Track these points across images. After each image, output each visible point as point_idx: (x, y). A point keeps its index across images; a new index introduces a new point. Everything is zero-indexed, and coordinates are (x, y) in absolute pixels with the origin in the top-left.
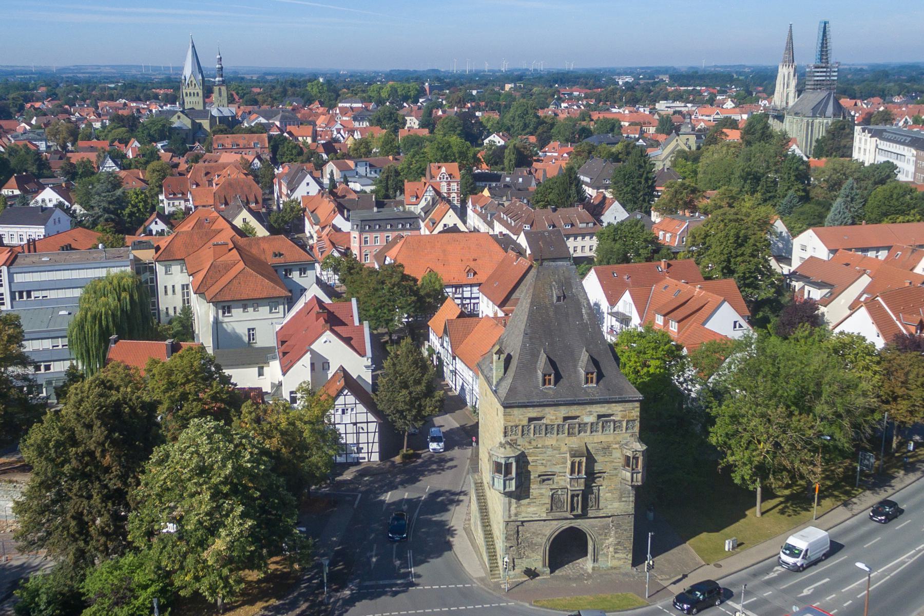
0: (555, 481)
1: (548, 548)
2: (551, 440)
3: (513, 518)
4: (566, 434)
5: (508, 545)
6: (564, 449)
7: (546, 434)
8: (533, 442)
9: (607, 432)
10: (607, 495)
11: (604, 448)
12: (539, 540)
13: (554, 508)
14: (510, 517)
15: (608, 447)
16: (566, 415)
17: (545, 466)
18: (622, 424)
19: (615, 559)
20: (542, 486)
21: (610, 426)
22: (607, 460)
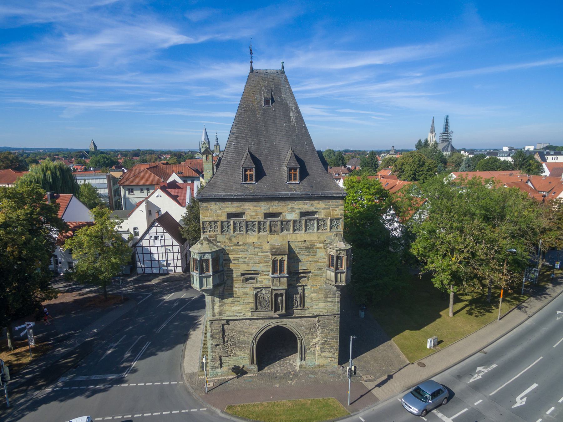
0: (259, 280)
1: (255, 346)
2: (252, 238)
3: (217, 317)
4: (268, 232)
5: (214, 343)
6: (267, 247)
7: (247, 231)
9: (311, 231)
10: (312, 295)
11: (307, 247)
12: (246, 338)
13: (259, 307)
14: (214, 316)
15: (313, 246)
16: (267, 211)
17: (248, 265)
18: (326, 223)
20: (245, 285)
21: (313, 224)
22: (311, 260)
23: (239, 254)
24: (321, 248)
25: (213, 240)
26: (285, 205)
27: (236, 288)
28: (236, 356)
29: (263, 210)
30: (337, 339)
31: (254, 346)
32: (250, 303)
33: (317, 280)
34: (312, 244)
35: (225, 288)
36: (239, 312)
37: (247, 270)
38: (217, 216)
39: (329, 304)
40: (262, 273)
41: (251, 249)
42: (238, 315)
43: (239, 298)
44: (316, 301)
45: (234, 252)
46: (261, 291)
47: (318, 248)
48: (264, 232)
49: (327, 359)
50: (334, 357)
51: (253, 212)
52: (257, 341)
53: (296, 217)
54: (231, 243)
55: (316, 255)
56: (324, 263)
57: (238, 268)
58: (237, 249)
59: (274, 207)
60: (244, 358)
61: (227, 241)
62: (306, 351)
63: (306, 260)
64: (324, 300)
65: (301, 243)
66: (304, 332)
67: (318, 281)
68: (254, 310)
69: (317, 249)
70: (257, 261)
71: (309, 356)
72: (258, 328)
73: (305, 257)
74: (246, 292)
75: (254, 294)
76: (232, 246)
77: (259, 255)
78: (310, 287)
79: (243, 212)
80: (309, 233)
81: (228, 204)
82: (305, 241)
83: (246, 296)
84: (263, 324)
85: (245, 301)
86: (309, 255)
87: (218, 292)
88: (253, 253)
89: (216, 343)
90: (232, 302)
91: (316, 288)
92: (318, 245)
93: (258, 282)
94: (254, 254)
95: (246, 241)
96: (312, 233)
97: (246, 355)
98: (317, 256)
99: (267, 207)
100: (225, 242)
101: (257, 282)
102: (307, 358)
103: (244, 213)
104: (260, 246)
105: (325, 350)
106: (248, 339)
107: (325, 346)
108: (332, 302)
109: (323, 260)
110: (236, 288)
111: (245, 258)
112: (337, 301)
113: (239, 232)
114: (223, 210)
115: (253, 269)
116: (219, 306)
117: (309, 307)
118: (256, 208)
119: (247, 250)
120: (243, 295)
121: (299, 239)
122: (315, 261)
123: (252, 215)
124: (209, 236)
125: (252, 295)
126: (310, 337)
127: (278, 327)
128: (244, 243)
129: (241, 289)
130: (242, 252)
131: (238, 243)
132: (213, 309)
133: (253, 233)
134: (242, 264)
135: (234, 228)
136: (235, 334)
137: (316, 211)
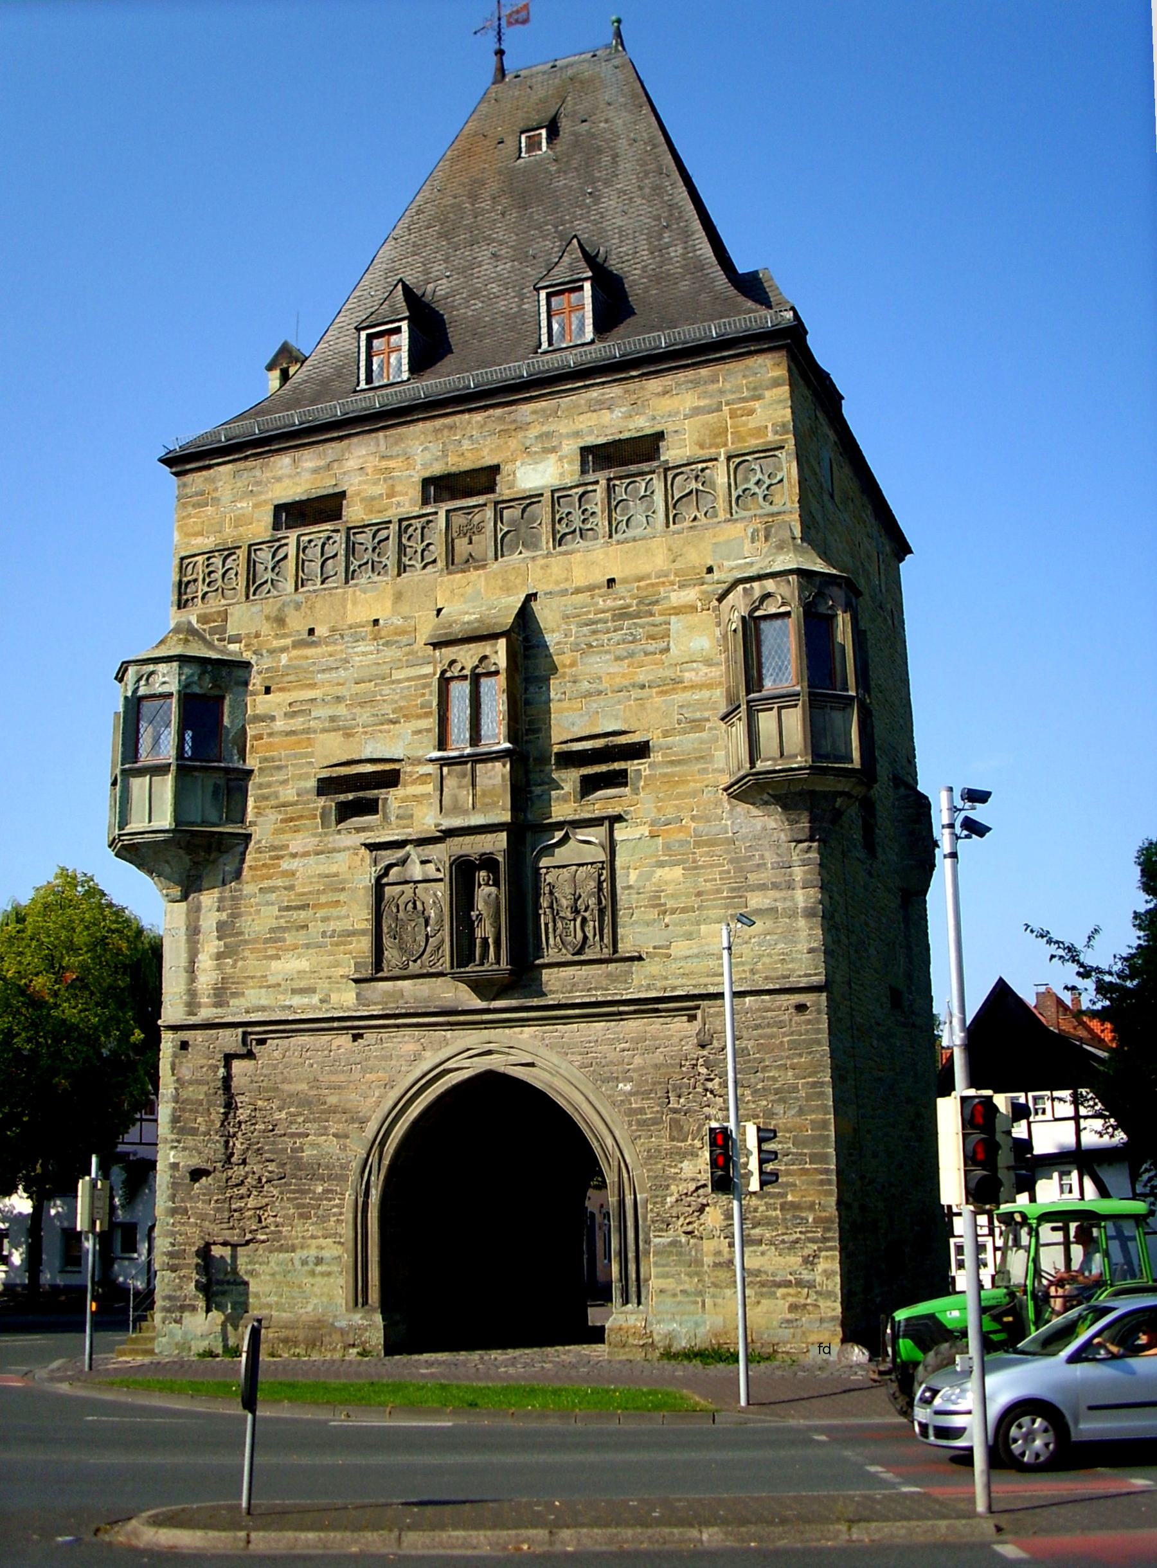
3: (206, 1013)
4: (441, 564)
8: (290, 612)
10: (659, 872)
11: (622, 614)
12: (331, 1145)
15: (648, 604)
16: (437, 469)
17: (348, 735)
22: (642, 677)
23: (313, 686)
24: (693, 609)
25: (213, 631)
26: (513, 427)
27: (294, 856)
28: (281, 1249)
29: (418, 467)
30: (823, 1158)
31: (373, 1191)
32: (353, 933)
34: (645, 594)
35: (248, 858)
36: (303, 984)
37: (344, 759)
38: (238, 522)
40: (409, 769)
41: (364, 654)
42: (297, 1001)
44: (684, 910)
45: (291, 678)
46: (403, 862)
47: (678, 611)
48: (424, 567)
49: (773, 1295)
50: (811, 1285)
51: (376, 483)
52: (386, 1162)
53: (562, 474)
54: (284, 636)
55: (667, 650)
56: (709, 686)
57: (307, 755)
58: (304, 662)
59: (466, 445)
60: (319, 1261)
61: (266, 629)
62: (648, 1242)
64: (727, 907)
65: (592, 596)
66: (632, 1112)
68: (368, 972)
69: (673, 619)
70: (387, 709)
71: (665, 1276)
72: (389, 1085)
73: (615, 668)
74: (336, 875)
75: (373, 881)
76: (284, 649)
77: (399, 681)
78: (645, 830)
79: (337, 490)
80: (626, 541)
81: (284, 462)
82: (611, 582)
84: (417, 1058)
85: (333, 925)
86: (631, 655)
88: (375, 671)
89: (196, 1162)
91: (681, 836)
92: (673, 596)
93: (393, 819)
94: (377, 677)
95: (344, 616)
96: (644, 538)
99: (435, 448)
100: (257, 636)
101: (386, 817)
102: (654, 1284)
103: (343, 494)
104: (404, 632)
105: (757, 1231)
106: (343, 1148)
108: (772, 911)
109: (705, 669)
110: (294, 856)
111: (339, 699)
112: (801, 905)
113: (319, 586)
114: (261, 493)
115: (366, 754)
116: (219, 956)
117: (646, 949)
118: (392, 464)
120: (324, 892)
121: (580, 578)
123: (373, 499)
124: (198, 616)
125: (362, 892)
126: (666, 1144)
127: (490, 1079)
128: (333, 630)
129: (312, 860)
131: (311, 631)
132: (191, 970)
133: (376, 578)
134: (324, 730)
135: (300, 565)
136: (283, 1115)
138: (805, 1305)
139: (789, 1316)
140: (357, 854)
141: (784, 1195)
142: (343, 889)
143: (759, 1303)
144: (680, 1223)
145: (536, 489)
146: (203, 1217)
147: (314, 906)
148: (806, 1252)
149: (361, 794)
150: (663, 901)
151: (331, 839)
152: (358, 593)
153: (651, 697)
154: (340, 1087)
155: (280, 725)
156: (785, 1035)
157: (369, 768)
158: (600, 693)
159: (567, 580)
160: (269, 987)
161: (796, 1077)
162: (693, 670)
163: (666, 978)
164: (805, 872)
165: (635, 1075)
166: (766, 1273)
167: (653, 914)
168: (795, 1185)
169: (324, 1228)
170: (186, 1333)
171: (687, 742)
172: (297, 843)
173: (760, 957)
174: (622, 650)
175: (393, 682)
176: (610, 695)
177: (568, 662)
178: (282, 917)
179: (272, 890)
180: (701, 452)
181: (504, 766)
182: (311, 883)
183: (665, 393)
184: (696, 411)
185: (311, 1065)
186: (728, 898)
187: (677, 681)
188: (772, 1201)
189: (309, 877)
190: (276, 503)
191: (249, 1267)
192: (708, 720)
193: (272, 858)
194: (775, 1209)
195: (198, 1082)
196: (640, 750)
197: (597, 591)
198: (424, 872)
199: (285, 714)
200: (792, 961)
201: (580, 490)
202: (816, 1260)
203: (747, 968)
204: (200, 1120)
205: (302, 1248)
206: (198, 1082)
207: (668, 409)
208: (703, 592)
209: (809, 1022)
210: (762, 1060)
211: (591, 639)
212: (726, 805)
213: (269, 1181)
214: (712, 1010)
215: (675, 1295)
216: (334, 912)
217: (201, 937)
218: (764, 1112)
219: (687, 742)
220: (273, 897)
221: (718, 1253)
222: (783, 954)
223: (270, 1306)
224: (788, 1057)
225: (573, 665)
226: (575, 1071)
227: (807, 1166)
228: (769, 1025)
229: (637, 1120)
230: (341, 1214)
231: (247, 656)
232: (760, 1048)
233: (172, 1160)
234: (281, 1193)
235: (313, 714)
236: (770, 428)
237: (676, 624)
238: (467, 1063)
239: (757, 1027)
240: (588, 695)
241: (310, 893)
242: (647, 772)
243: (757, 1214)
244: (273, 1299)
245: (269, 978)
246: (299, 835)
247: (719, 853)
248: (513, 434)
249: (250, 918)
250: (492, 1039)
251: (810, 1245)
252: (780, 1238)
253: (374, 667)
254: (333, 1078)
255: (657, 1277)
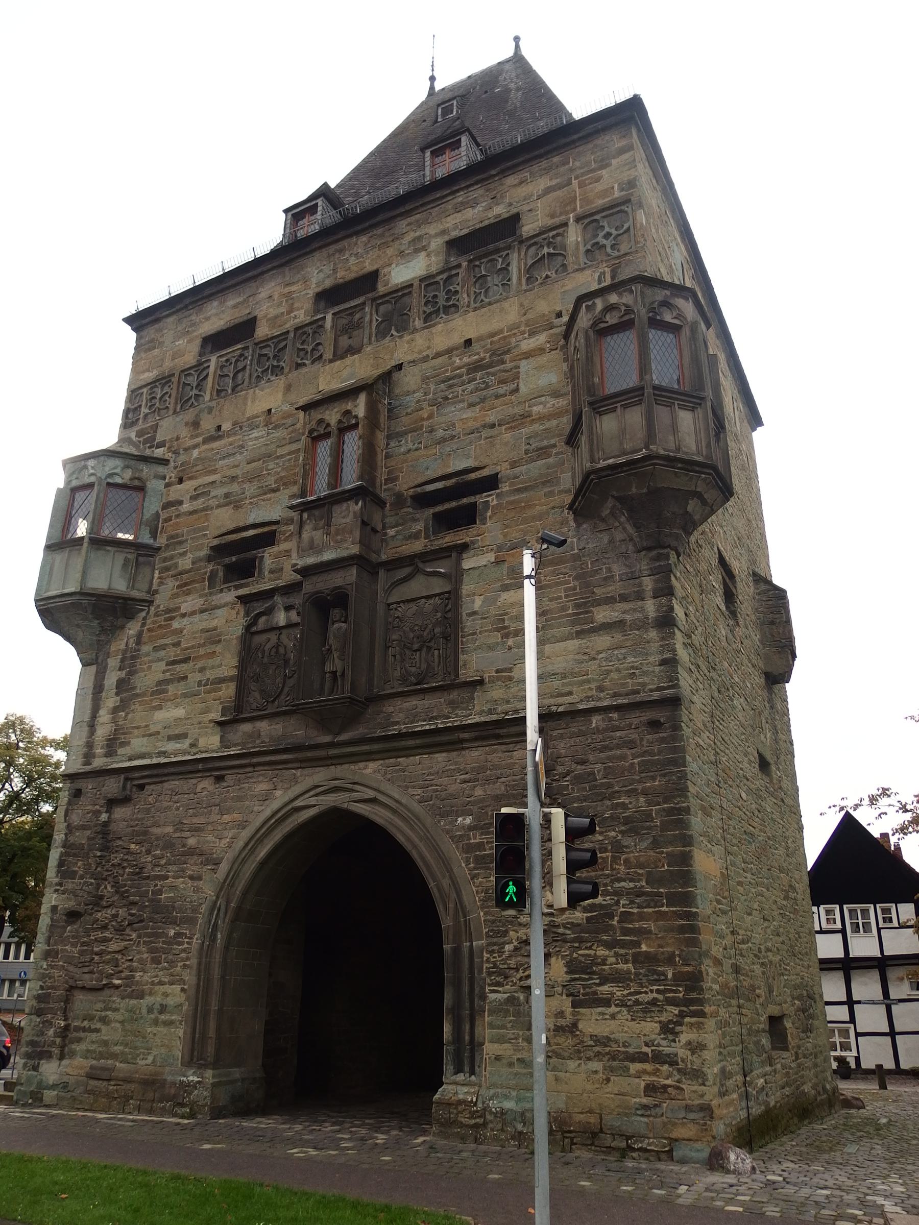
3: (98, 763)
11: (475, 367)
17: (237, 508)
19: (578, 1053)
21: (505, 269)
22: (492, 418)
23: (214, 472)
27: (184, 615)
28: (130, 996)
32: (222, 680)
33: (529, 513)
34: (497, 346)
35: (149, 621)
39: (603, 641)
41: (257, 438)
42: (171, 746)
43: (186, 660)
45: (198, 468)
46: (269, 612)
47: (527, 355)
48: (313, 363)
50: (671, 1061)
54: (197, 436)
55: (517, 390)
59: (353, 260)
61: (184, 432)
62: (483, 997)
63: (472, 424)
64: (573, 623)
66: (468, 849)
67: (534, 518)
71: (500, 1040)
72: (242, 825)
73: (468, 414)
74: (215, 629)
76: (195, 446)
77: (282, 456)
79: (250, 317)
82: (468, 343)
83: (213, 648)
86: (483, 400)
87: (123, 646)
88: (263, 451)
89: (71, 904)
90: (159, 683)
93: (266, 573)
97: (175, 995)
98: (523, 389)
99: (328, 270)
100: (178, 438)
102: (490, 1049)
103: (255, 317)
105: (605, 988)
107: (602, 952)
109: (551, 402)
114: (194, 331)
118: (293, 288)
119: (242, 447)
120: (203, 645)
122: (513, 418)
125: (235, 642)
127: (335, 815)
128: (235, 424)
129: (197, 618)
130: (224, 458)
134: (219, 506)
137: (514, 211)
138: (665, 1087)
139: (645, 1101)
140: (233, 608)
141: (637, 944)
142: (219, 641)
143: (608, 1080)
144: (518, 976)
145: (408, 281)
146: (69, 960)
147: (195, 658)
148: (664, 1018)
149: (242, 556)
150: (507, 623)
151: (214, 598)
152: (257, 391)
153: (501, 433)
154: (198, 830)
155: (186, 507)
156: (635, 756)
157: (251, 532)
158: (453, 437)
159: (429, 348)
160: (150, 735)
161: (649, 803)
162: (541, 403)
163: (508, 702)
164: (656, 581)
165: (475, 809)
166: (616, 1042)
167: (497, 637)
168: (650, 932)
169: (172, 975)
170: (40, 1083)
171: (536, 468)
172: (189, 603)
173: (608, 672)
174: (474, 398)
175: (278, 457)
176: (462, 438)
177: (426, 415)
178: (168, 671)
179: (163, 647)
180: (553, 221)
181: (357, 504)
182: (194, 638)
183: (521, 183)
184: (548, 191)
185: (178, 809)
186: (574, 614)
187: (525, 416)
188: (622, 951)
189: (194, 633)
190: (203, 336)
191: (103, 1014)
192: (554, 446)
193: (166, 620)
194: (626, 962)
195: (83, 828)
196: (492, 483)
197: (455, 352)
198: (288, 618)
199: (191, 498)
200: (646, 673)
201: (444, 276)
202: (678, 1029)
203: (593, 686)
204: (80, 863)
205: (150, 994)
206: (83, 828)
207: (523, 194)
208: (552, 335)
209: (662, 740)
210: (610, 786)
211: (447, 393)
212: (572, 524)
213: (129, 925)
214: (555, 733)
215: (511, 1065)
216: (210, 662)
217: (104, 694)
218: (611, 843)
219: (536, 468)
220: (163, 653)
221: (561, 1014)
222: (633, 668)
223: (114, 1056)
224: (639, 781)
225: (431, 416)
226: (415, 805)
227: (664, 909)
228: (618, 746)
229: (476, 856)
230: (188, 959)
231: (168, 456)
232: (608, 772)
233: (53, 903)
234: (139, 936)
235: (212, 494)
236: (616, 188)
237: (525, 366)
238: (313, 801)
239: (604, 749)
240: (443, 440)
241: (193, 647)
242: (495, 502)
243: (606, 967)
244: (117, 1049)
245: (151, 726)
246: (189, 598)
247: (564, 571)
248: (391, 244)
249: (143, 674)
250: (339, 775)
251: (669, 1008)
252: (633, 998)
253: (263, 449)
254: (195, 820)
255: (491, 1042)
